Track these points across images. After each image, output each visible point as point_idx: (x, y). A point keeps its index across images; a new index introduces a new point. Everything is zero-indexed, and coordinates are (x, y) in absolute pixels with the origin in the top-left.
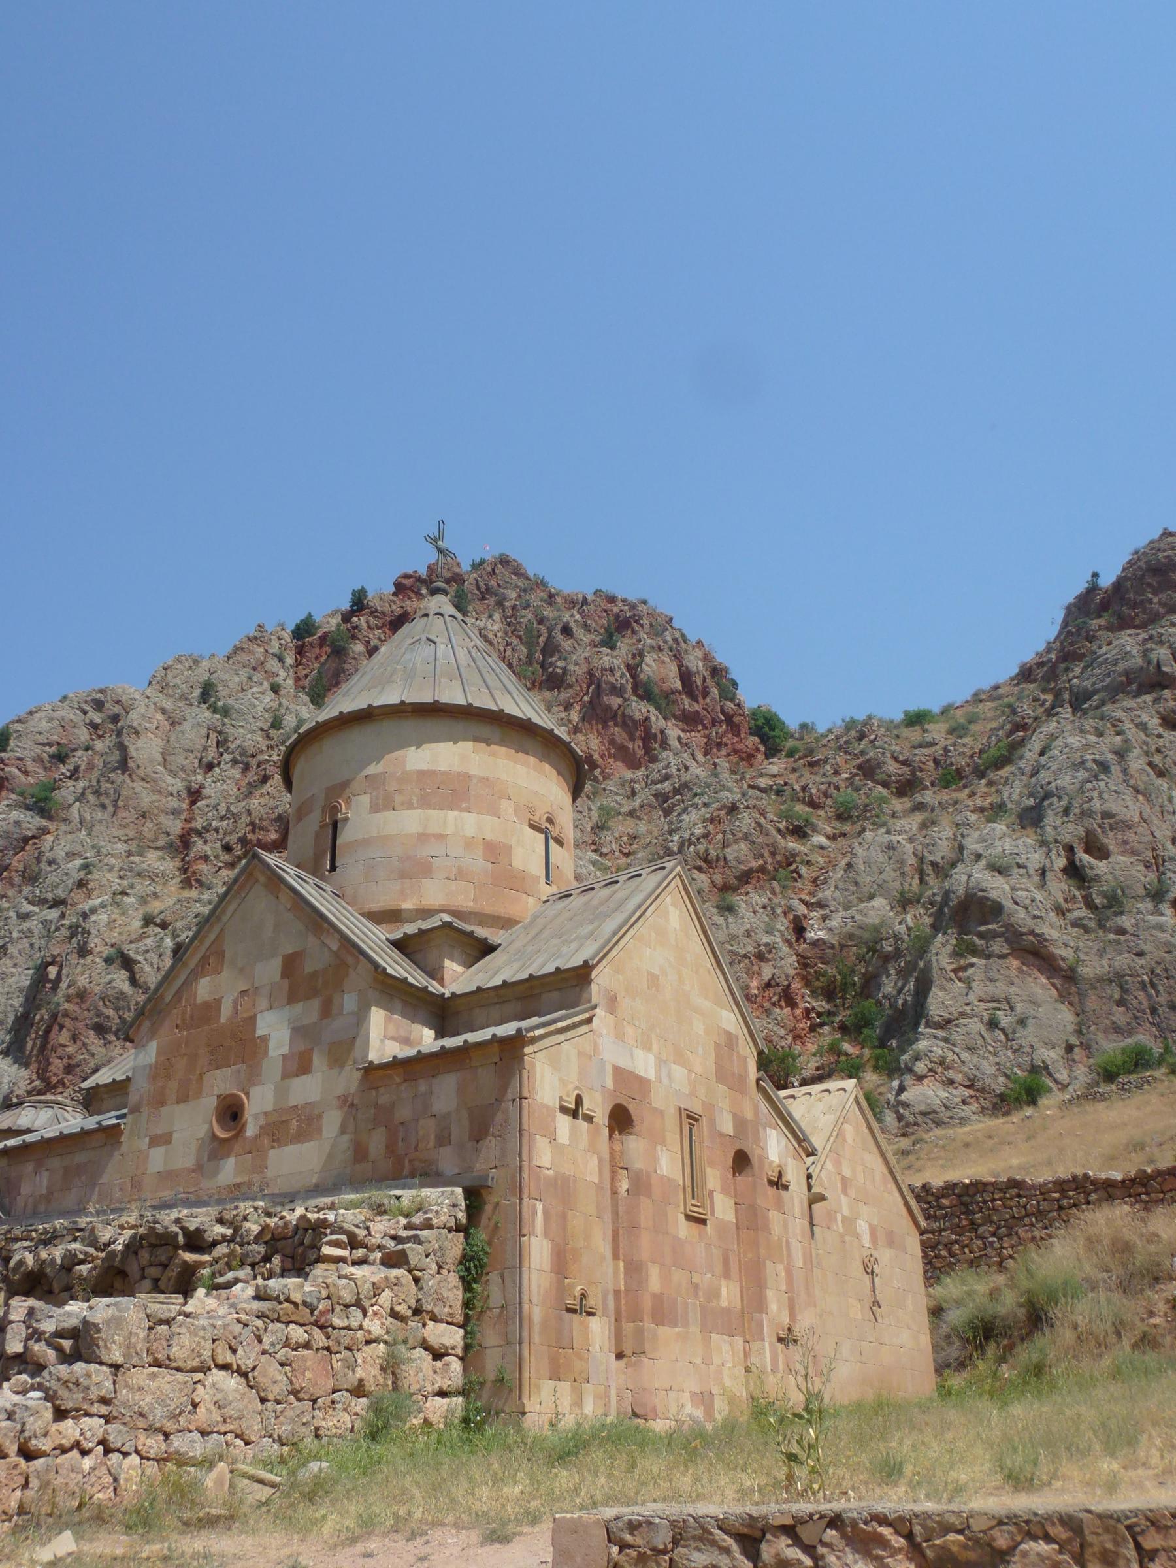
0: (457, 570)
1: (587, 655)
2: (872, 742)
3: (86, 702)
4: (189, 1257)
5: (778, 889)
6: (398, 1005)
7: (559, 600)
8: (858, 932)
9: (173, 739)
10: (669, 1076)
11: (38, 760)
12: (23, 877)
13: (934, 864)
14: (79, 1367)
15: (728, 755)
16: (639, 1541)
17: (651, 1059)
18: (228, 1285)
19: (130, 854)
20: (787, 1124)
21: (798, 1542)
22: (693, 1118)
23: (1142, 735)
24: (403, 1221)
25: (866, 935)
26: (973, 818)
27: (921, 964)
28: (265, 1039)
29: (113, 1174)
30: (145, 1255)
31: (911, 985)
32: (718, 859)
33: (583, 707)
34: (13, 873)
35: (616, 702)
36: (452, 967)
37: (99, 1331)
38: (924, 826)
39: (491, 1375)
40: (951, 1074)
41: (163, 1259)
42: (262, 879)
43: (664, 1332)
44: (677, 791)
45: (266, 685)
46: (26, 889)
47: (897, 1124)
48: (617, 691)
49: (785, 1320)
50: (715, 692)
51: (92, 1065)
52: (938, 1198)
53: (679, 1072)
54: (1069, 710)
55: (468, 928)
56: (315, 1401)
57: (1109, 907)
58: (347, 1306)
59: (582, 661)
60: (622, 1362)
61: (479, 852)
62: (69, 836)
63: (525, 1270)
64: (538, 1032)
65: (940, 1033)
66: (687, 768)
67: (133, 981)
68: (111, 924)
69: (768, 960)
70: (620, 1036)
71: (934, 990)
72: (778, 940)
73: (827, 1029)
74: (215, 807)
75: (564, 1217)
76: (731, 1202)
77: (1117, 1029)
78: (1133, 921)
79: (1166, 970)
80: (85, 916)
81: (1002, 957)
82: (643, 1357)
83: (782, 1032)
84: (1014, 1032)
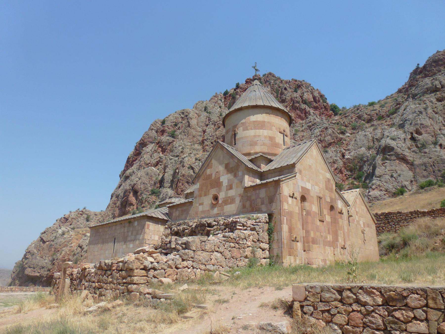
0: (259, 77)
2: (360, 110)
4: (208, 229)
5: (338, 147)
6: (251, 174)
7: (283, 82)
8: (358, 156)
9: (199, 119)
10: (314, 189)
11: (171, 126)
13: (376, 139)
14: (187, 251)
15: (325, 116)
16: (313, 291)
17: (310, 184)
18: (217, 234)
19: (191, 145)
20: (343, 199)
21: (352, 292)
22: (320, 198)
24: (254, 221)
25: (360, 157)
26: (386, 127)
27: (374, 163)
28: (222, 182)
29: (192, 211)
30: (199, 228)
31: (371, 168)
32: (323, 140)
33: (290, 107)
35: (298, 105)
36: (262, 165)
37: (190, 243)
38: (374, 130)
39: (275, 254)
40: (381, 188)
41: (203, 229)
42: (220, 147)
43: (315, 246)
44: (313, 125)
45: (218, 106)
46: (171, 153)
47: (368, 200)
48: (298, 102)
50: (321, 101)
52: (379, 216)
53: (317, 188)
54: (411, 99)
55: (266, 156)
56: (237, 259)
57: (422, 147)
58: (243, 239)
59: (289, 96)
60: (305, 252)
63: (282, 232)
64: (283, 179)
65: (378, 179)
67: (194, 172)
68: (188, 160)
69: (336, 163)
70: (302, 180)
71: (377, 169)
72: (338, 158)
73: (350, 179)
74: (209, 134)
75: (291, 220)
76: (330, 217)
77: (424, 177)
78: (428, 150)
80: (183, 159)
81: (394, 160)
82: (310, 251)
83: (340, 180)
84: (397, 178)
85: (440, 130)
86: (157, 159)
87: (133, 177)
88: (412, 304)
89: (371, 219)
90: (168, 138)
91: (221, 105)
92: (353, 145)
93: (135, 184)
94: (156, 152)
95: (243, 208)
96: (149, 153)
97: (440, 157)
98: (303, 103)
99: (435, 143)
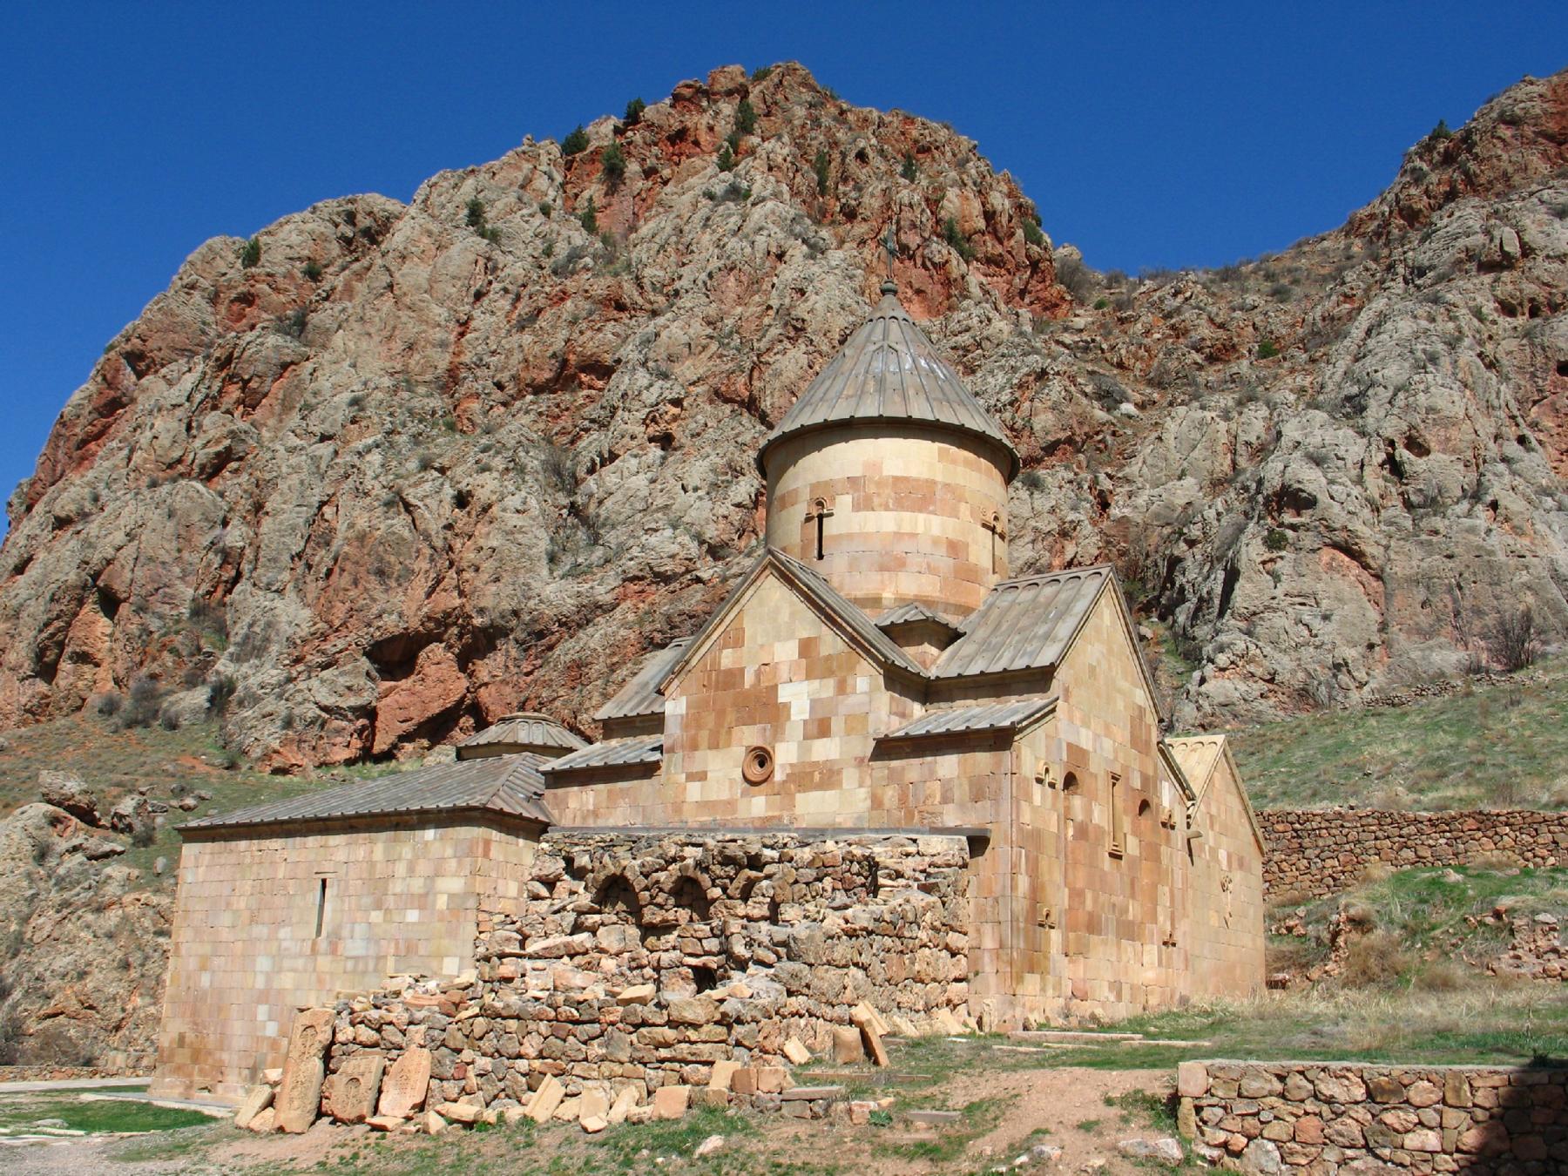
1: (884, 186)
2: (1186, 299)
3: (338, 214)
7: (851, 117)
12: (283, 405)
13: (1248, 444)
20: (1176, 776)
22: (1115, 778)
23: (1475, 321)
28: (787, 706)
34: (274, 402)
40: (1252, 668)
41: (732, 873)
43: (1094, 938)
45: (536, 207)
49: (1168, 928)
51: (375, 610)
53: (1107, 744)
54: (1402, 285)
59: (878, 192)
61: (943, 550)
62: (334, 367)
65: (1243, 625)
66: (989, 320)
70: (1071, 720)
77: (1419, 631)
79: (1475, 574)
81: (1314, 551)
85: (1496, 438)
86: (218, 442)
87: (93, 528)
88: (1416, 1100)
89: (1252, 839)
90: (273, 340)
91: (549, 200)
92: (1149, 461)
93: (109, 562)
94: (215, 408)
95: (873, 808)
96: (179, 413)
97: (1486, 558)
98: (938, 236)
99: (1475, 495)
